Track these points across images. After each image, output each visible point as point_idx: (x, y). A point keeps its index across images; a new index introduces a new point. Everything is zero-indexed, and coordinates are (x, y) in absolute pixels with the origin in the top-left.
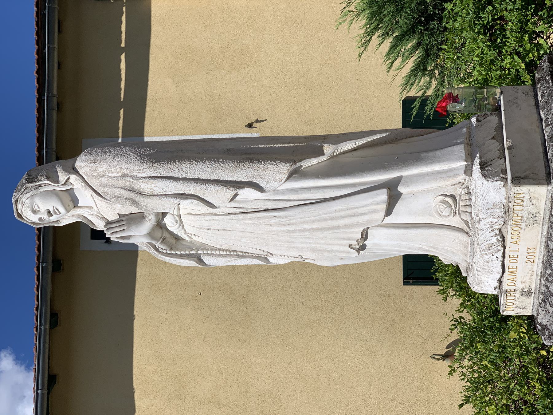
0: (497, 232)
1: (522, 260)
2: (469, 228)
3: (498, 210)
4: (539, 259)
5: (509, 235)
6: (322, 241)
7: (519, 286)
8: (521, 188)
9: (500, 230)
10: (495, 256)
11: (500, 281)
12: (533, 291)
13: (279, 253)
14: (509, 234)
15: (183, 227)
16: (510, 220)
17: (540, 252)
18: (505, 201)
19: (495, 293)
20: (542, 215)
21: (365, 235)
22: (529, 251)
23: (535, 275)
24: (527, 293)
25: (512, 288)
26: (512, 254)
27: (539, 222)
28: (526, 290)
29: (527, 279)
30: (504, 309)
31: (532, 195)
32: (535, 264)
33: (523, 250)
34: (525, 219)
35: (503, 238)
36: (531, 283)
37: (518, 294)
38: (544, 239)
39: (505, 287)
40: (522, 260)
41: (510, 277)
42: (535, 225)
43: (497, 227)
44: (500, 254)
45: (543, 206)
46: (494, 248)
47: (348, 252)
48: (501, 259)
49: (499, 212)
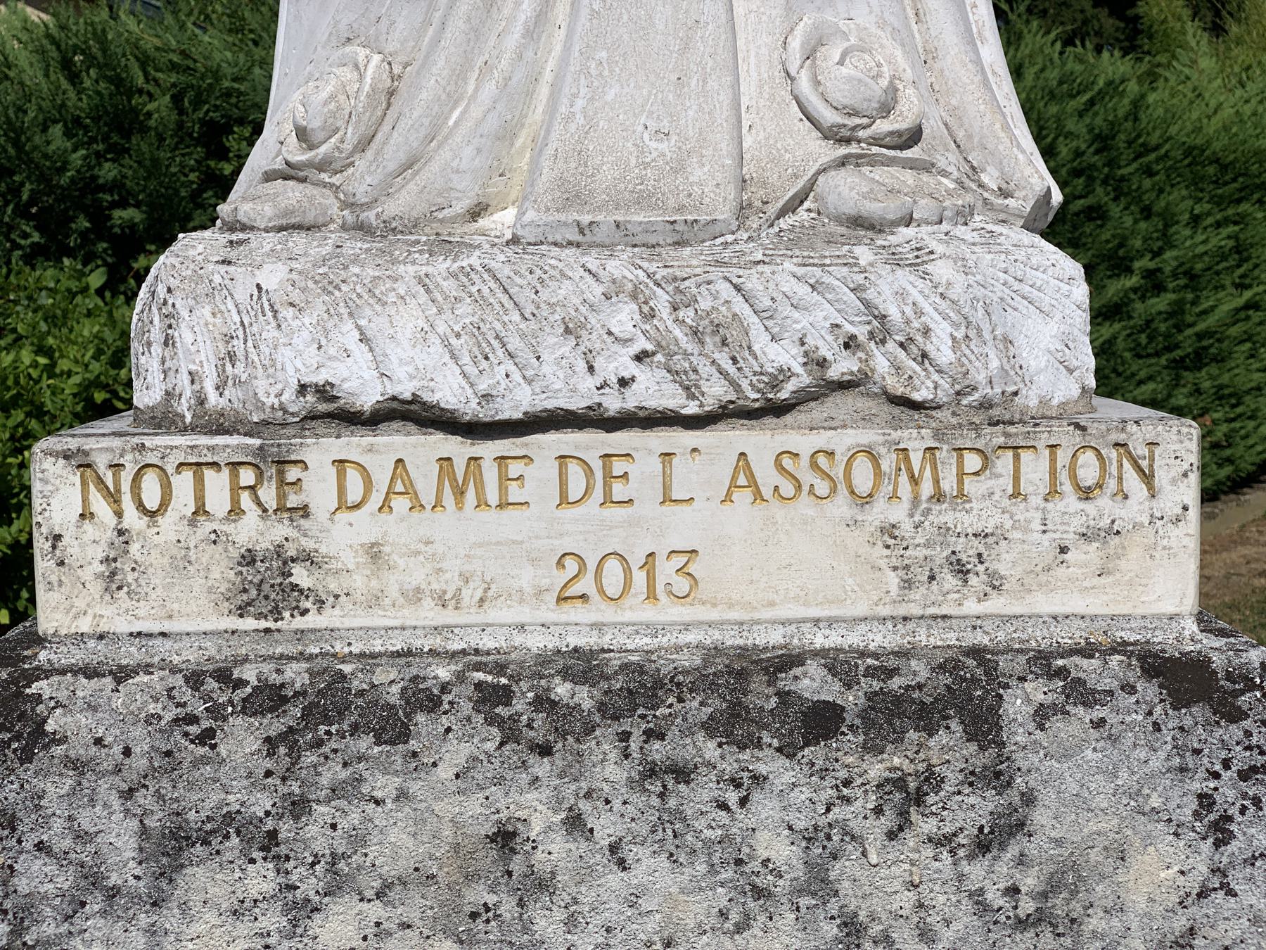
0: (843, 366)
1: (589, 527)
2: (782, 213)
3: (995, 363)
4: (598, 627)
5: (805, 443)
7: (340, 538)
8: (1194, 478)
10: (631, 369)
14: (821, 439)
16: (937, 435)
17: (654, 629)
18: (1033, 402)
19: (146, 395)
20: (972, 607)
22: (666, 570)
23: (448, 617)
24: (269, 585)
27: (917, 594)
28: (300, 576)
30: (101, 462)
32: (549, 612)
33: (681, 528)
34: (948, 518)
35: (777, 410)
36: (375, 601)
37: (253, 530)
39: (321, 452)
41: (425, 479)
42: (893, 580)
43: (881, 364)
44: (654, 391)
45: (1044, 604)
48: (613, 404)
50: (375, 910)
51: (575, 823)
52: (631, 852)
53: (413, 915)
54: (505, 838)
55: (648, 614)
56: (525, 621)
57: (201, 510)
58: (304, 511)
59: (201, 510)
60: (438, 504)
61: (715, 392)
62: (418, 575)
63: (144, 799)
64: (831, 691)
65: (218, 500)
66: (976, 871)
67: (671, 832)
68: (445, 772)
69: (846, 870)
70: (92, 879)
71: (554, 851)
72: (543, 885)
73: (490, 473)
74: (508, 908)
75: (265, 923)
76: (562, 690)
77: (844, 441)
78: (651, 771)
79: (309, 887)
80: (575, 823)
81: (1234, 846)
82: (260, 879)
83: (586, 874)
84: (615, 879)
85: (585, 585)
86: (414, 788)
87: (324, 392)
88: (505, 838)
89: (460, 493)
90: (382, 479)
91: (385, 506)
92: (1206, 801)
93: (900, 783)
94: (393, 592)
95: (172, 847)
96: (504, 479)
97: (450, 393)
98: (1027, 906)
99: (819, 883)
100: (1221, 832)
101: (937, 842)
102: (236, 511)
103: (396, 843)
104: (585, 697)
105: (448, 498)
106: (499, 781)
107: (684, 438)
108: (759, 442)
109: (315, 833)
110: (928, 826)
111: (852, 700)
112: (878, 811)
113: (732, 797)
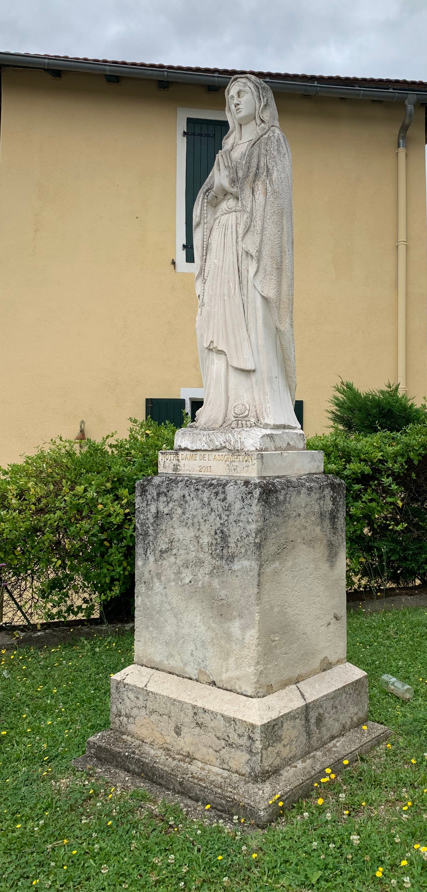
0: (223, 445)
1: (202, 463)
5: (221, 454)
6: (216, 321)
9: (225, 447)
10: (204, 444)
11: (186, 449)
12: (177, 473)
13: (206, 288)
15: (226, 214)
20: (235, 475)
21: (221, 352)
22: (209, 468)
23: (190, 473)
24: (176, 468)
25: (180, 458)
26: (207, 456)
28: (178, 467)
29: (187, 467)
31: (250, 468)
33: (210, 463)
37: (175, 462)
38: (217, 477)
39: (180, 453)
40: (202, 463)
41: (188, 456)
42: (228, 471)
44: (206, 447)
45: (242, 475)
46: (211, 444)
47: (207, 341)
49: (238, 446)
50: (174, 503)
52: (194, 499)
54: (184, 496)
56: (196, 473)
61: (211, 448)
66: (222, 503)
71: (188, 498)
77: (224, 454)
80: (189, 495)
82: (165, 499)
83: (190, 501)
84: (192, 502)
88: (184, 496)
92: (242, 497)
93: (216, 493)
97: (189, 447)
99: (209, 504)
101: (220, 500)
107: (210, 453)
108: (217, 453)
110: (218, 498)
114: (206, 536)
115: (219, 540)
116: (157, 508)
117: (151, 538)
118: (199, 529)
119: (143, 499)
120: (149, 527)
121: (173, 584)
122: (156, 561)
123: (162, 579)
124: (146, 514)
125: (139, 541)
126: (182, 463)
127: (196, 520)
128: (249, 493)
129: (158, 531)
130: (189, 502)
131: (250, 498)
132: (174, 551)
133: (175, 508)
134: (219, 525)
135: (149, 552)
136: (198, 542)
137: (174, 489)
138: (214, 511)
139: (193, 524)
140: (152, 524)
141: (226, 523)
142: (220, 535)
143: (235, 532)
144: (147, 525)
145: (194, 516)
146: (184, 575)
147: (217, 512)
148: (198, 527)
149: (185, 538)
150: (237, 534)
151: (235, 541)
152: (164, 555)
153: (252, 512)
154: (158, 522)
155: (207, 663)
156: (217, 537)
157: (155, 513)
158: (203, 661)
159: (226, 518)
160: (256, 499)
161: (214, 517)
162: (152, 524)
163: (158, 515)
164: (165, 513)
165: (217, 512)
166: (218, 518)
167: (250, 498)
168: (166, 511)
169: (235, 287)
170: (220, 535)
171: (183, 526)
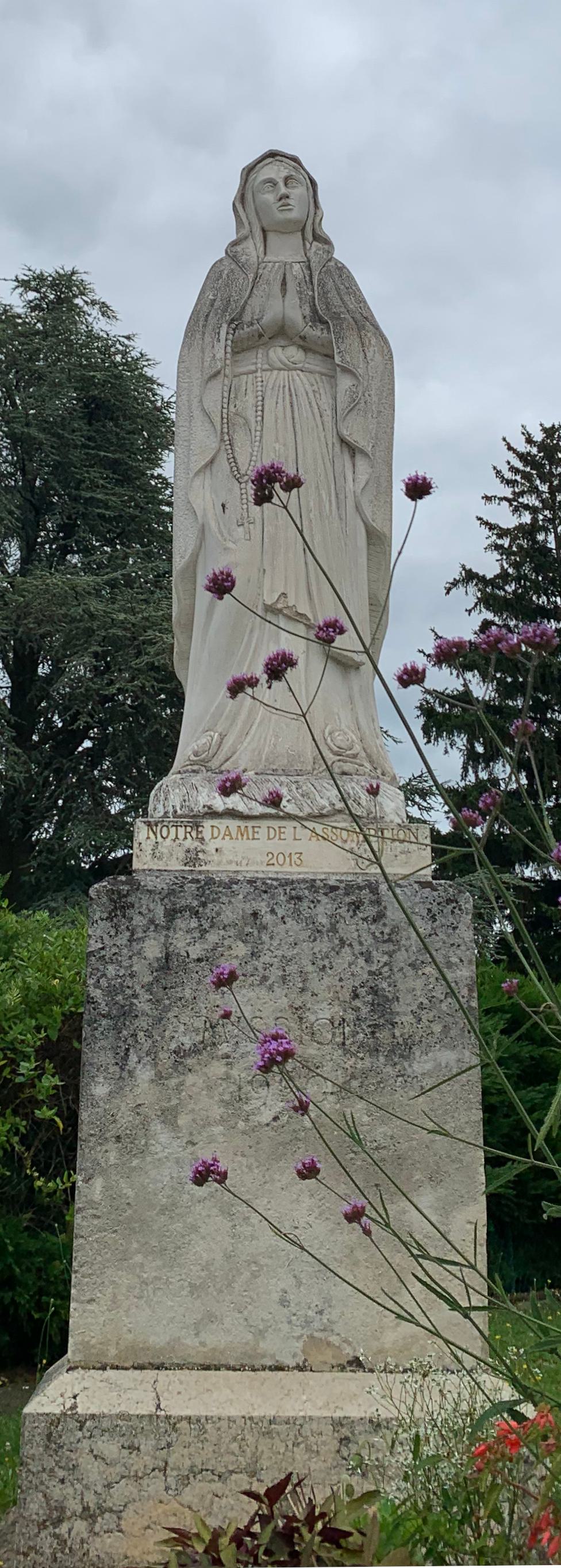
4: (277, 873)
22: (295, 857)
23: (238, 868)
24: (192, 858)
28: (201, 855)
29: (228, 856)
33: (298, 847)
37: (189, 843)
39: (208, 824)
50: (222, 932)
51: (273, 911)
52: (286, 919)
53: (232, 934)
54: (255, 915)
55: (289, 869)
57: (177, 838)
58: (203, 839)
59: (177, 838)
60: (237, 839)
62: (231, 858)
63: (166, 900)
64: (338, 884)
65: (181, 835)
66: (373, 927)
67: (297, 913)
68: (241, 896)
69: (340, 926)
70: (152, 921)
71: (268, 918)
72: (265, 928)
73: (250, 830)
74: (256, 933)
75: (194, 935)
76: (269, 882)
78: (292, 898)
79: (206, 926)
80: (273, 911)
81: (437, 923)
82: (194, 923)
85: (274, 861)
86: (233, 900)
87: (209, 808)
88: (255, 915)
89: (242, 835)
90: (222, 833)
91: (223, 838)
92: (429, 910)
93: (353, 903)
94: (224, 861)
95: (171, 914)
96: (254, 832)
98: (386, 937)
99: (333, 929)
100: (433, 918)
101: (365, 919)
102: (186, 838)
103: (228, 915)
104: (275, 883)
105: (240, 837)
106: (254, 899)
109: (210, 909)
110: (361, 915)
111: (343, 885)
112: (348, 911)
113: (312, 906)
114: (325, 1005)
115: (365, 1010)
116: (166, 946)
117: (143, 1023)
118: (303, 990)
119: (116, 927)
120: (135, 996)
121: (218, 1129)
122: (160, 1078)
123: (180, 1122)
124: (124, 964)
125: (97, 1034)
126: (211, 847)
127: (292, 968)
128: (449, 901)
129: (167, 1002)
130: (271, 928)
131: (453, 912)
132: (224, 1048)
133: (226, 943)
134: (366, 976)
135: (133, 1058)
136: (301, 1019)
137: (224, 899)
138: (350, 945)
139: (284, 979)
140: (148, 988)
141: (386, 969)
142: (369, 998)
143: (412, 989)
144: (129, 992)
145: (287, 960)
146: (255, 1103)
147: (357, 948)
148: (300, 985)
149: (258, 1014)
150: (419, 993)
151: (414, 1008)
152: (189, 1061)
153: (457, 941)
154: (171, 980)
155: (335, 1314)
156: (357, 1003)
157: (158, 959)
158: (321, 1312)
159: (386, 958)
160: (467, 914)
161: (350, 958)
162: (148, 988)
163: (167, 963)
164: (194, 956)
165: (357, 948)
166: (361, 961)
167: (453, 912)
168: (196, 951)
169: (330, 501)
170: (369, 998)
171: (252, 985)
